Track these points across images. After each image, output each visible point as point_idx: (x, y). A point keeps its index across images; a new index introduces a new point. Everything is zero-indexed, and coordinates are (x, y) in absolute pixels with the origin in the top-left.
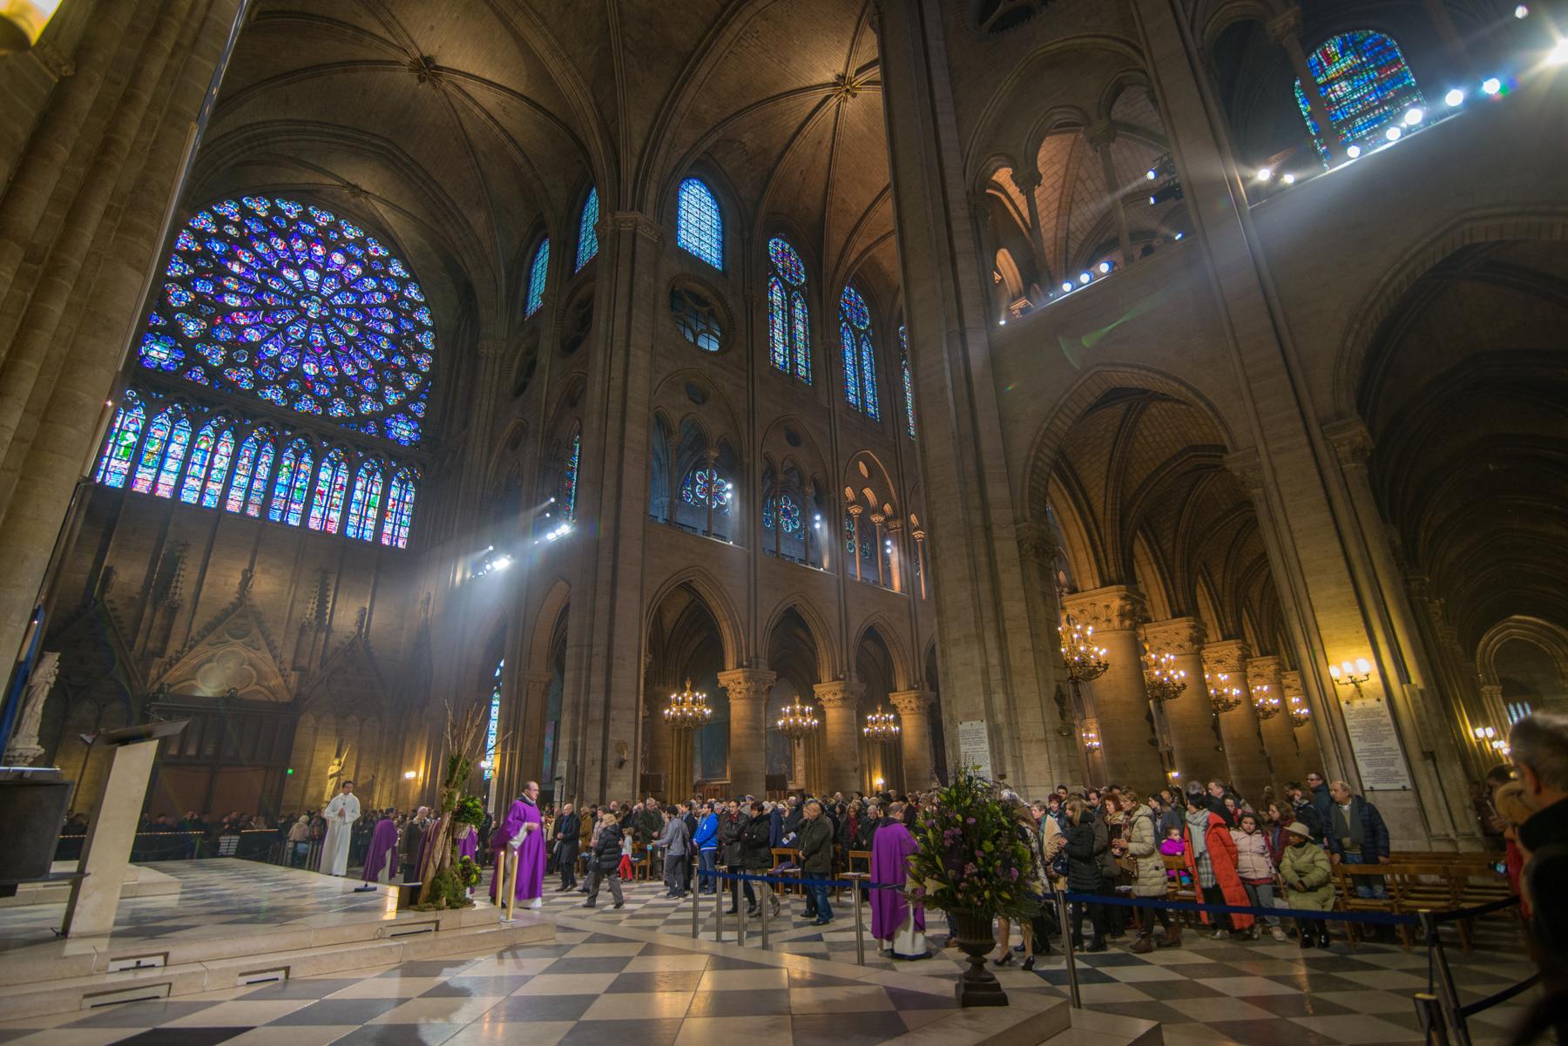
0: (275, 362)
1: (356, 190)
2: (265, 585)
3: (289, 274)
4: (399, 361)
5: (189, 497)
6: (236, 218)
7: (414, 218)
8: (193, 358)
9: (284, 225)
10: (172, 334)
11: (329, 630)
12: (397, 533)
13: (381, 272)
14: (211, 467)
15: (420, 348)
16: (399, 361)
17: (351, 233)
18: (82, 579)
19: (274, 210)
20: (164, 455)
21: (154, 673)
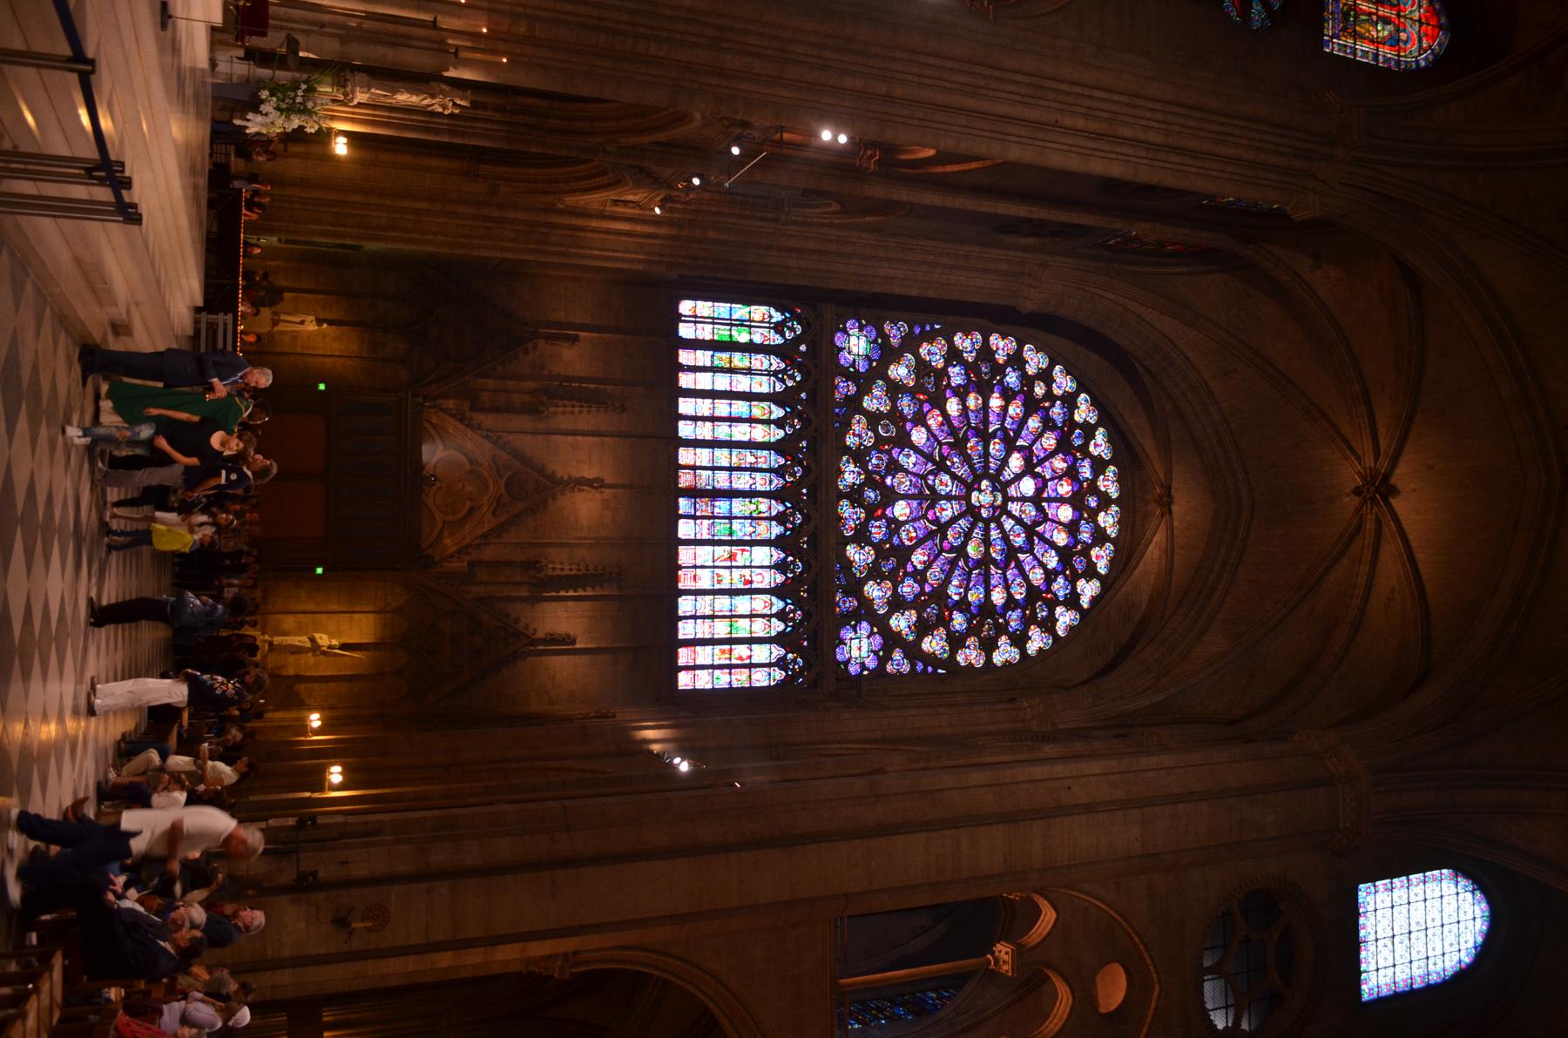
0: (894, 467)
1: (1166, 502)
2: (585, 509)
3: (1016, 462)
4: (958, 621)
5: (686, 406)
6: (1057, 391)
7: (1169, 570)
8: (864, 382)
9: (1078, 442)
10: (886, 354)
11: (534, 600)
12: (699, 673)
13: (1074, 570)
14: (732, 420)
15: (989, 646)
16: (958, 621)
17: (1107, 520)
18: (561, 316)
19: (1089, 431)
20: (732, 371)
21: (451, 404)
